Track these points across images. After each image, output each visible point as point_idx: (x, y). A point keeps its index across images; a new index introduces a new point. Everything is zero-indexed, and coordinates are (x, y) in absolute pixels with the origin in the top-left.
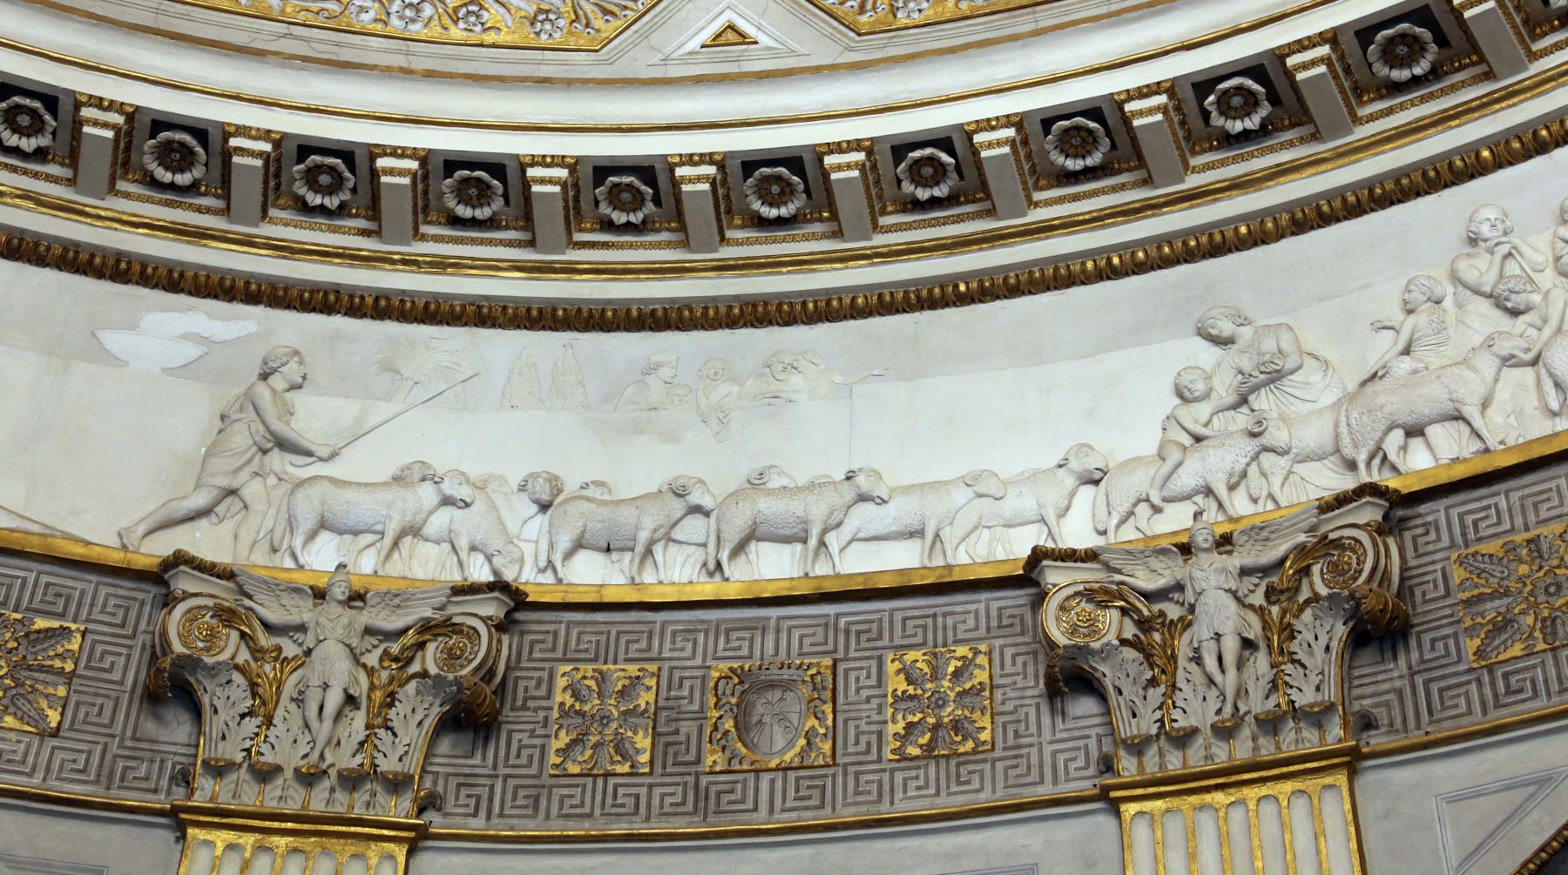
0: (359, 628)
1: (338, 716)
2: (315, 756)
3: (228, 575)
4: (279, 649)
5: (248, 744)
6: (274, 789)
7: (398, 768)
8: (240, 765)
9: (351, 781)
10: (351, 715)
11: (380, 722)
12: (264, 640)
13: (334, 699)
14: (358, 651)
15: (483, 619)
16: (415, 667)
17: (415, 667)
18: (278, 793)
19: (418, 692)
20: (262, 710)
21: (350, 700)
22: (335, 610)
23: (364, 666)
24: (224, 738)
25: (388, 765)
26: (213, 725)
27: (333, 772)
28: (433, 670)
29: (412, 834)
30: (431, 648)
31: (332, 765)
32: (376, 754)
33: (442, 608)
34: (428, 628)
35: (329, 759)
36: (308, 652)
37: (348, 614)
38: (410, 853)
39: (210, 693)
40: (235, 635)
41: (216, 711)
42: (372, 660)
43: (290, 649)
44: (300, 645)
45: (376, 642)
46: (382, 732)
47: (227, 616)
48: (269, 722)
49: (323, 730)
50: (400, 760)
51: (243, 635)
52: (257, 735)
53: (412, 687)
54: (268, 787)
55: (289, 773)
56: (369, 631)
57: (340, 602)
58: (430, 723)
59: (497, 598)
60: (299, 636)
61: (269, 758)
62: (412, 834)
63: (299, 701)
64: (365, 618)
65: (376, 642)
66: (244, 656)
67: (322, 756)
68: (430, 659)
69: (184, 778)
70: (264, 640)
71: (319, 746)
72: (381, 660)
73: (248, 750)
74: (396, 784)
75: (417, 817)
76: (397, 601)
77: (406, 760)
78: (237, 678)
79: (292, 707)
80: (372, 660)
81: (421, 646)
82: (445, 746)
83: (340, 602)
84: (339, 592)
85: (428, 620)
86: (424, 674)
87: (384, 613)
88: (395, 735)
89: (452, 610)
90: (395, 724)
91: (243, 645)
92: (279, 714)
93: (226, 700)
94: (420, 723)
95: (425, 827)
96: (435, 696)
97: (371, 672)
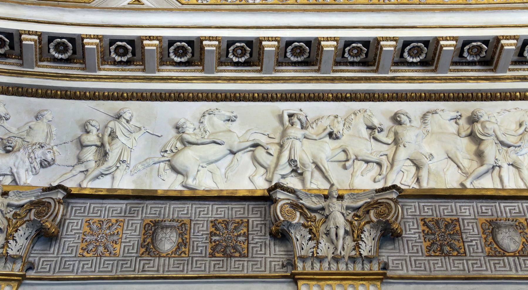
6: (326, 265)
9: (353, 260)
13: (341, 232)
21: (346, 233)
24: (303, 249)
26: (297, 245)
28: (375, 220)
30: (372, 213)
34: (368, 207)
37: (340, 202)
40: (298, 214)
41: (297, 240)
42: (349, 218)
44: (323, 215)
47: (295, 206)
48: (318, 243)
51: (301, 214)
52: (314, 247)
56: (348, 208)
63: (327, 234)
76: (355, 197)
79: (324, 236)
80: (349, 218)
85: (369, 202)
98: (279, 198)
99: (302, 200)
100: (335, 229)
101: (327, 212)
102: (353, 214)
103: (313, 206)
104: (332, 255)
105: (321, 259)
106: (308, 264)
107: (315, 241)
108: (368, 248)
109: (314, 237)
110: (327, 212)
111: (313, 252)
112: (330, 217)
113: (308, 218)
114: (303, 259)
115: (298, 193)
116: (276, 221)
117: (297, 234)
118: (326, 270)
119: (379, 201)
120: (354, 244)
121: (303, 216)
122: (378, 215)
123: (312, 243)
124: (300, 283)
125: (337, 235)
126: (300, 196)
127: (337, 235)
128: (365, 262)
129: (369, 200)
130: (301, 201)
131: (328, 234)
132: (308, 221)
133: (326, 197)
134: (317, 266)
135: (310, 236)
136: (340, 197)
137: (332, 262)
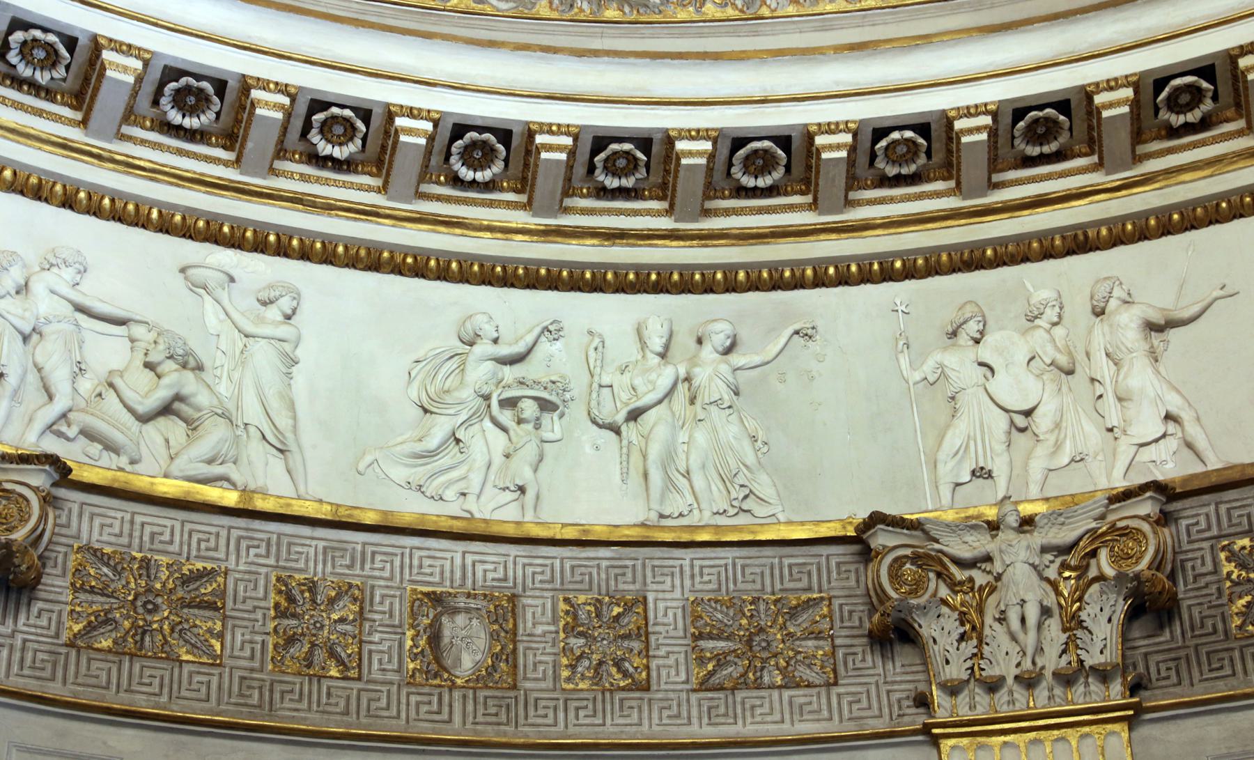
0: (1038, 550)
1: (1040, 626)
2: (1027, 664)
3: (915, 526)
4: (971, 580)
5: (969, 664)
7: (1102, 659)
8: (968, 681)
9: (1066, 679)
10: (1047, 623)
11: (1073, 624)
12: (959, 574)
13: (1032, 614)
14: (1040, 568)
15: (1145, 518)
16: (1093, 573)
17: (1093, 573)
18: (1006, 698)
19: (1102, 592)
20: (972, 632)
21: (1046, 612)
22: (1012, 535)
23: (1048, 580)
24: (947, 662)
25: (1093, 658)
26: (936, 651)
27: (1048, 674)
28: (1110, 572)
29: (1131, 712)
30: (1103, 554)
31: (1043, 668)
32: (1079, 652)
33: (1102, 517)
35: (1039, 664)
36: (998, 578)
37: (1025, 539)
38: (1130, 729)
39: (928, 628)
40: (932, 575)
42: (1052, 573)
43: (980, 578)
44: (989, 572)
45: (1052, 558)
46: (1079, 633)
49: (1030, 640)
50: (1102, 652)
52: (975, 655)
53: (1095, 587)
54: (997, 696)
55: (1010, 681)
56: (1044, 550)
57: (1014, 529)
58: (1119, 616)
59: (1151, 497)
60: (987, 566)
61: (991, 672)
62: (1131, 712)
63: (1002, 619)
64: (1038, 538)
65: (1052, 558)
66: (944, 592)
67: (1034, 663)
68: (1105, 563)
69: (923, 702)
70: (959, 574)
71: (1030, 652)
72: (1060, 574)
73: (972, 668)
74: (1103, 675)
75: (1131, 696)
76: (1061, 519)
77: (1107, 652)
78: (945, 610)
79: (996, 625)
81: (1094, 554)
82: (1136, 633)
83: (1014, 529)
84: (1012, 520)
85: (1094, 530)
86: (1101, 578)
87: (1054, 530)
88: (1090, 632)
89: (1111, 518)
90: (1088, 623)
91: (940, 582)
92: (987, 631)
93: (940, 631)
94: (1110, 620)
95: (1139, 703)
96: (1119, 594)
97: (1054, 585)
98: (884, 547)
99: (937, 541)
100: (1018, 607)
101: (998, 567)
102: (1059, 560)
103: (965, 553)
104: (1017, 672)
105: (993, 686)
106: (963, 698)
107: (975, 642)
108: (1100, 645)
109: (972, 632)
110: (998, 567)
111: (972, 668)
112: (1004, 578)
113: (955, 585)
114: (953, 689)
115: (928, 527)
116: (881, 602)
117: (934, 626)
118: (1005, 711)
119: (1120, 524)
120: (1064, 637)
121: (945, 581)
122: (1115, 559)
123: (969, 647)
124: (946, 744)
125: (1023, 620)
126: (933, 533)
127: (1023, 620)
128: (1090, 680)
129: (1093, 525)
130: (937, 546)
131: (1004, 619)
132: (956, 593)
133: (994, 527)
134: (982, 699)
135: (962, 630)
136: (1027, 523)
137: (1016, 687)
